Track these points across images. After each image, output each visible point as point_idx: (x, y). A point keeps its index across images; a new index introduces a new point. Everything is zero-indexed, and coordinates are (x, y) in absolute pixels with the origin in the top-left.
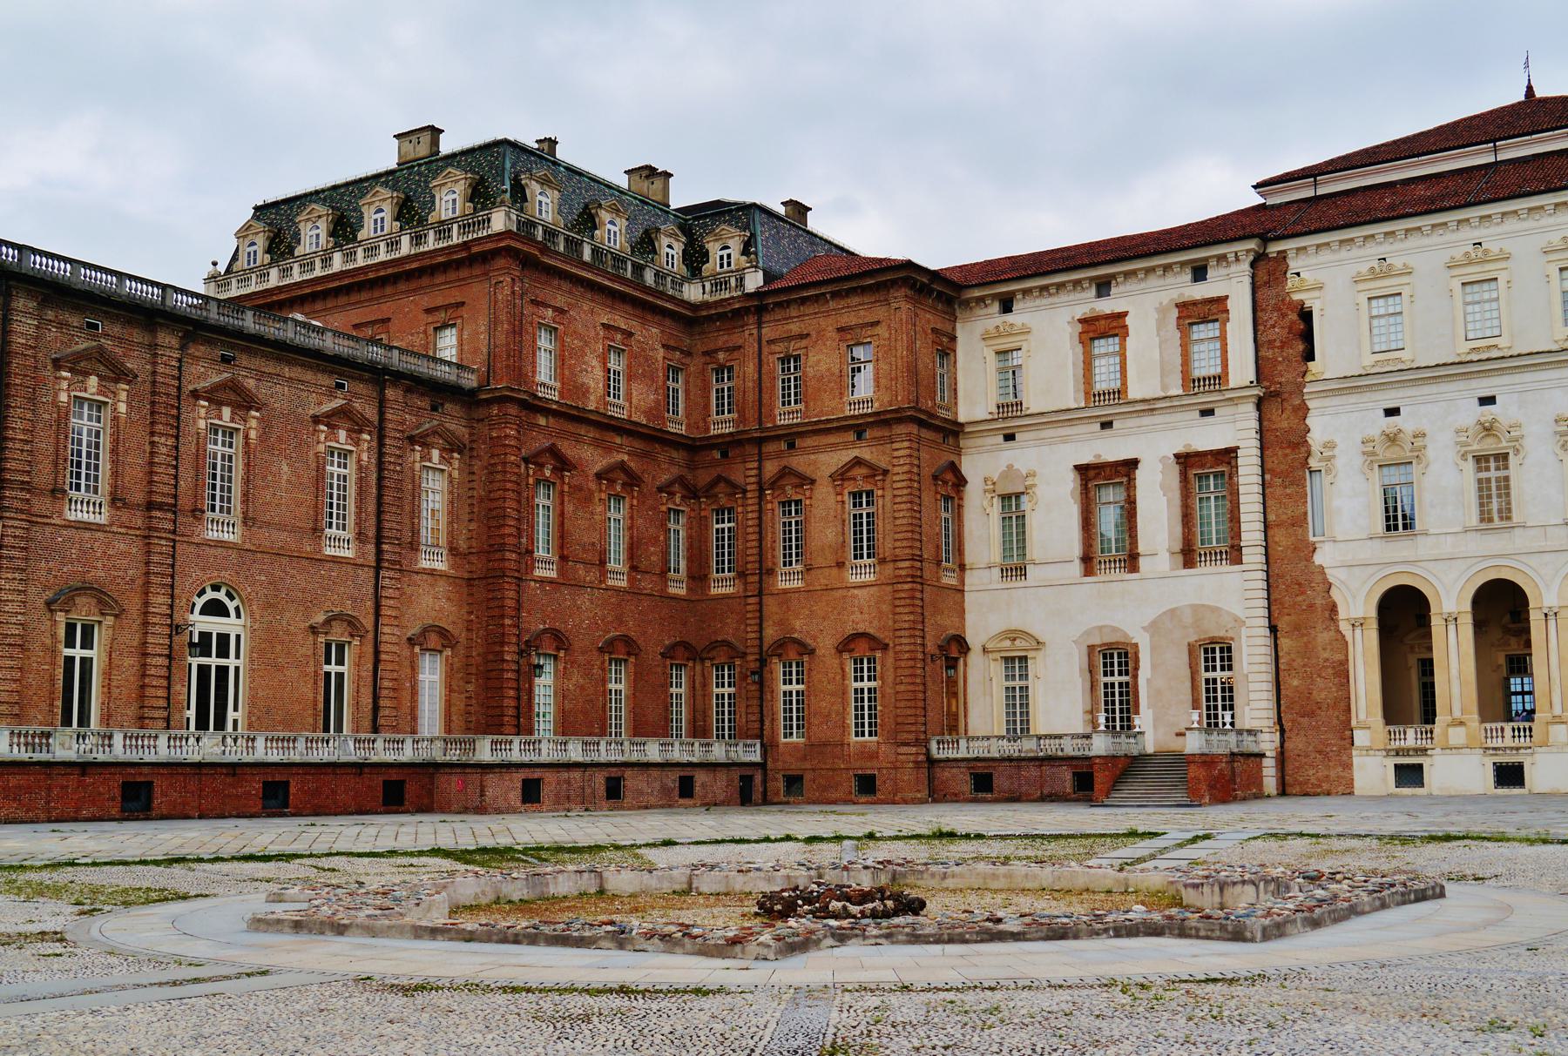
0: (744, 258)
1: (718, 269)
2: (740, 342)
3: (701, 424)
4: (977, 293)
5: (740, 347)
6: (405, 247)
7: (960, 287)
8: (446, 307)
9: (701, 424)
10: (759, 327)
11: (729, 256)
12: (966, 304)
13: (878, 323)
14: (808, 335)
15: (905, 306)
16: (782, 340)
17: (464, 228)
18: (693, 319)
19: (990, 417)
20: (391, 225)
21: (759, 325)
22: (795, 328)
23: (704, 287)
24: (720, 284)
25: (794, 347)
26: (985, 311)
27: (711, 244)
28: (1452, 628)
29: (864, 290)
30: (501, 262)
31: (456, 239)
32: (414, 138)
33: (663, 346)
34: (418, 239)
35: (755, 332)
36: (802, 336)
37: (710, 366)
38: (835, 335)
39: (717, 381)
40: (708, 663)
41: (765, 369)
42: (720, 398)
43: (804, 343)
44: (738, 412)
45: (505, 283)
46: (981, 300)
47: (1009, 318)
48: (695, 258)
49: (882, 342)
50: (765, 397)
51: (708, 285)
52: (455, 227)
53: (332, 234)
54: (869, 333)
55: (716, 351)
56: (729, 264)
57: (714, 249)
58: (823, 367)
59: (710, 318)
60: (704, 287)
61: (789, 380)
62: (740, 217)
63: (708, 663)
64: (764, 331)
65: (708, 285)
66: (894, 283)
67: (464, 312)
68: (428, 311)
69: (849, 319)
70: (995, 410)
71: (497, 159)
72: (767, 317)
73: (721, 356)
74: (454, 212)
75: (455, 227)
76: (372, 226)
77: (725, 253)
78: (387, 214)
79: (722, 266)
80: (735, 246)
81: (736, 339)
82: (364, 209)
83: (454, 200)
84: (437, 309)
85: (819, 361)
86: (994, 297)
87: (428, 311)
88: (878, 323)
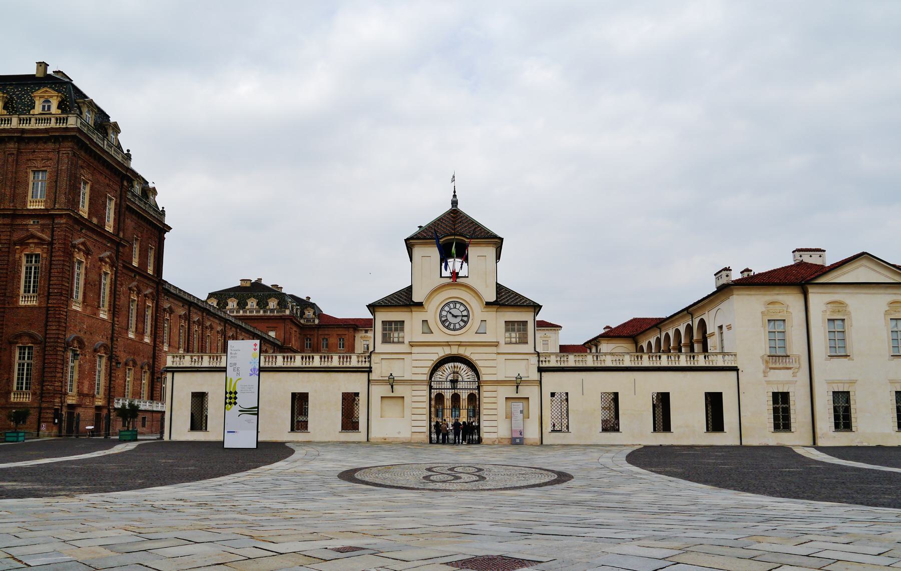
5: (312, 335)
6: (262, 313)
7: (357, 327)
8: (273, 327)
12: (358, 330)
13: (345, 335)
14: (329, 335)
15: (352, 332)
17: (277, 312)
18: (302, 328)
20: (255, 306)
21: (318, 331)
22: (326, 332)
24: (308, 320)
25: (326, 337)
31: (275, 314)
34: (265, 312)
36: (328, 335)
42: (307, 345)
45: (289, 325)
46: (361, 330)
47: (366, 334)
48: (303, 313)
55: (307, 335)
57: (307, 313)
68: (267, 327)
69: (339, 333)
73: (308, 336)
78: (255, 304)
80: (311, 313)
87: (267, 327)
88: (345, 335)
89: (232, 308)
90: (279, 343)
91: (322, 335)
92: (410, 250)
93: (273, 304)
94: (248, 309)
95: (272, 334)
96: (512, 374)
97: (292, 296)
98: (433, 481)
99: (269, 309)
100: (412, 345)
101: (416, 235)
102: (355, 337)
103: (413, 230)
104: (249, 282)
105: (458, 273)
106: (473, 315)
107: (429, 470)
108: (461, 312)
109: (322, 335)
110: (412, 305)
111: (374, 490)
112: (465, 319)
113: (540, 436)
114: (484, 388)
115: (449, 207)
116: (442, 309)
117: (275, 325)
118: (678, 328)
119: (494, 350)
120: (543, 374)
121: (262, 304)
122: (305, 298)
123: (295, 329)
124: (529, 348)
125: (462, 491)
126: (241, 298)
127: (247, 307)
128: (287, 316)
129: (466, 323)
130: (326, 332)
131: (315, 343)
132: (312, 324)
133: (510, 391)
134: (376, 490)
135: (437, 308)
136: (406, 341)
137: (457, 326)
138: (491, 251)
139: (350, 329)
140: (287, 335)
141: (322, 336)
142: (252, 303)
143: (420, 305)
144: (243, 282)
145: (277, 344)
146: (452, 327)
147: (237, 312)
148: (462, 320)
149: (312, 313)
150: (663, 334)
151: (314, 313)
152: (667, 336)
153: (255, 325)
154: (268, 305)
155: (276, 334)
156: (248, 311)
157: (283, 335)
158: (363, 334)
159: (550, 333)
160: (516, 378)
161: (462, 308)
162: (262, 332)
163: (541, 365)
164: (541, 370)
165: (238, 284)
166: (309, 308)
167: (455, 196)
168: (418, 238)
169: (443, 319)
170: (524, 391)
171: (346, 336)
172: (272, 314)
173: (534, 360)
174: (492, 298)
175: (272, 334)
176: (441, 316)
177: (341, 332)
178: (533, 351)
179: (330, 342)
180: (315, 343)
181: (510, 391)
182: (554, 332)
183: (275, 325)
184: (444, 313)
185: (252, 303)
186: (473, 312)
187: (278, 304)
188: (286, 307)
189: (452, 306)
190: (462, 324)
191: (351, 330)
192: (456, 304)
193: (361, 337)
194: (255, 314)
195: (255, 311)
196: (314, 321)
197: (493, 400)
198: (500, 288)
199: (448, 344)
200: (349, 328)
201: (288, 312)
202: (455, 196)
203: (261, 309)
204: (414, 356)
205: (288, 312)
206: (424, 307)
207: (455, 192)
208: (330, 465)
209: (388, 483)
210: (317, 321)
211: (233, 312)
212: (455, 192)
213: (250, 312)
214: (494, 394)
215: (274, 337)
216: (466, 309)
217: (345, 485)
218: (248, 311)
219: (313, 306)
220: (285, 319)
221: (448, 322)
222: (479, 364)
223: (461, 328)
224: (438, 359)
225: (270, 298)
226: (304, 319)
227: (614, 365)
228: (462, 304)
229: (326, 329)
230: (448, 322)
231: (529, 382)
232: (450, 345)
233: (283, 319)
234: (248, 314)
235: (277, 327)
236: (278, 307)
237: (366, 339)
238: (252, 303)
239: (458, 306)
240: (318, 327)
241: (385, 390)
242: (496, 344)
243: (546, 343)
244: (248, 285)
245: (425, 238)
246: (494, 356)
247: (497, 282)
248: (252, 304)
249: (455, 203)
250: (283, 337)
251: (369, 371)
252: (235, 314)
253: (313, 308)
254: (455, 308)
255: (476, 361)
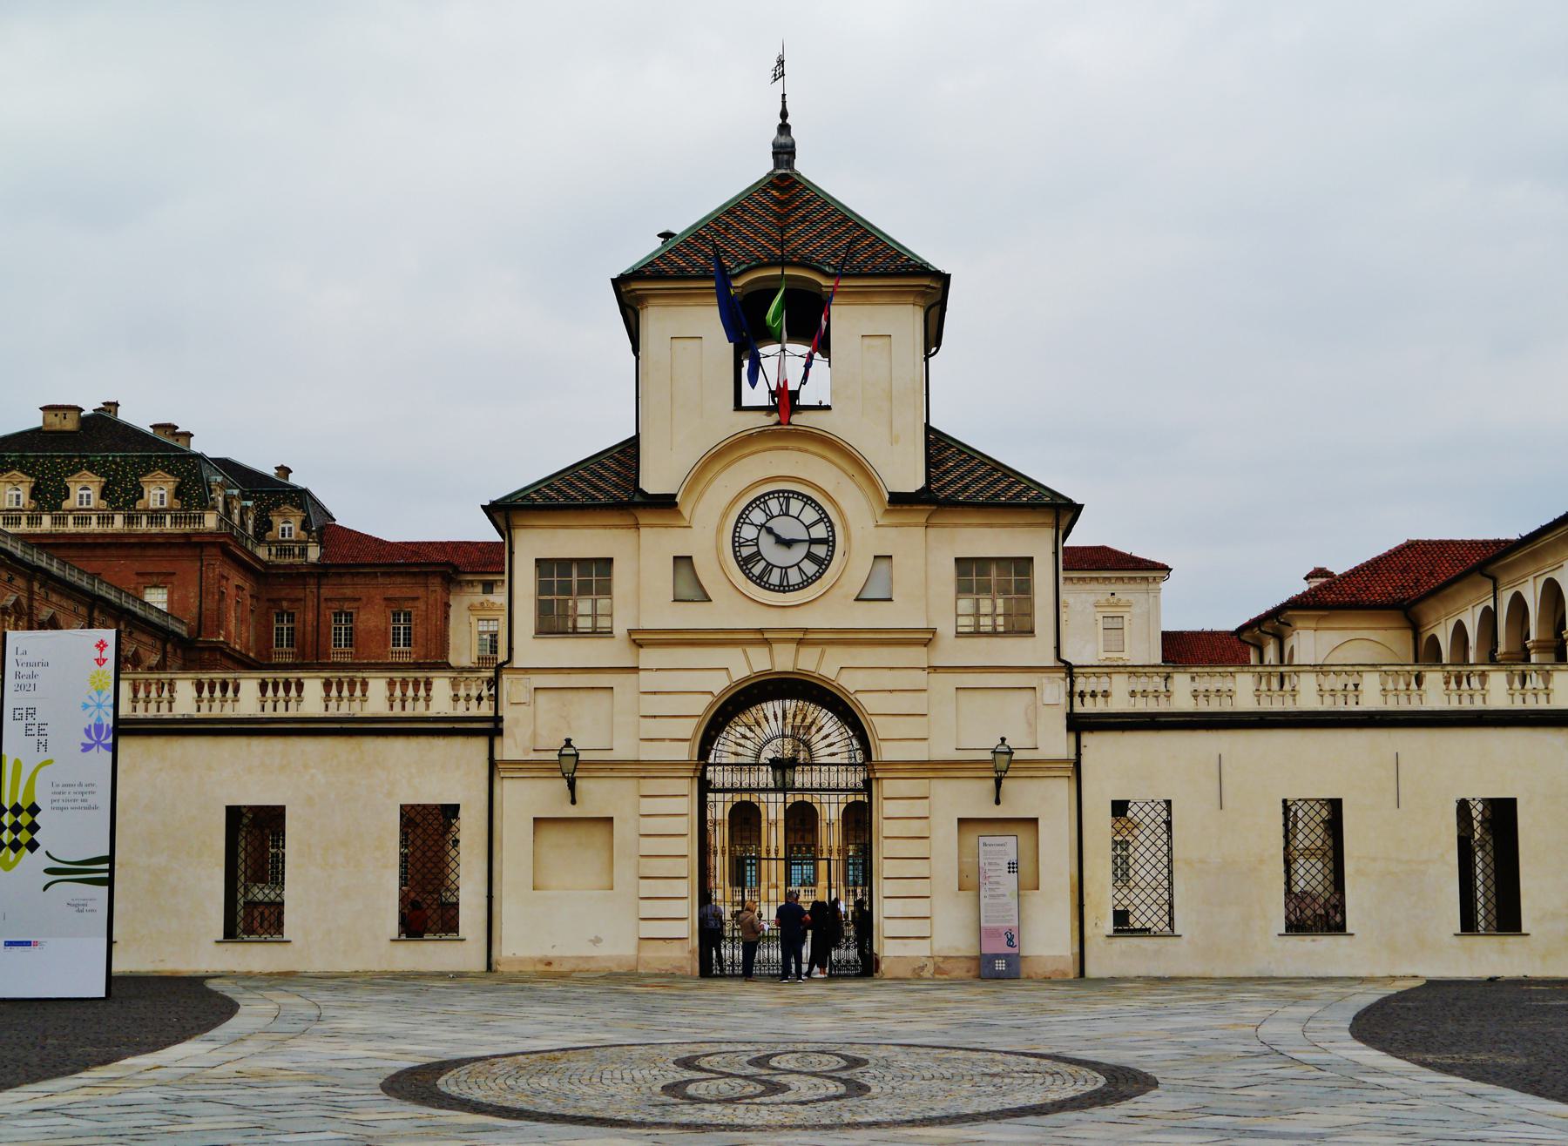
0: (302, 533)
1: (280, 537)
2: (302, 595)
3: (264, 653)
4: (469, 578)
5: (301, 600)
6: (119, 523)
7: (457, 570)
8: (159, 574)
9: (264, 653)
10: (319, 588)
11: (290, 529)
12: (459, 583)
13: (418, 598)
14: (360, 599)
15: (439, 589)
16: (338, 600)
17: (175, 521)
18: (261, 575)
19: (472, 665)
20: (95, 501)
21: (319, 587)
22: (348, 592)
23: (270, 550)
24: (284, 550)
25: (347, 606)
26: (471, 590)
27: (275, 518)
28: (774, 829)
29: (408, 574)
30: (214, 551)
31: (168, 526)
32: (60, 414)
33: (251, 596)
34: (130, 520)
35: (315, 590)
37: (274, 610)
38: (381, 602)
39: (277, 621)
40: (267, 831)
41: (322, 619)
43: (355, 604)
44: (298, 648)
45: (218, 567)
46: (471, 582)
47: (491, 598)
48: (264, 525)
49: (420, 613)
50: (322, 639)
51: (274, 550)
52: (168, 518)
53: (33, 496)
54: (410, 605)
55: (280, 600)
56: (290, 535)
57: (278, 523)
58: (372, 624)
59: (278, 576)
60: (270, 550)
61: (340, 629)
62: (294, 497)
63: (267, 831)
64: (322, 591)
65: (274, 550)
66: (434, 574)
67: (174, 579)
68: (138, 574)
69: (393, 592)
70: (477, 661)
71: (194, 468)
72: (324, 581)
73: (285, 604)
74: (162, 503)
75: (168, 518)
76: (78, 500)
77: (287, 526)
78: (94, 492)
79: (283, 535)
80: (294, 524)
81: (299, 593)
82: (71, 486)
83: (162, 496)
84: (150, 574)
85: (369, 619)
86: (480, 581)
87: (138, 574)
88: (418, 598)
89: (14, 506)
90: (183, 631)
91: (331, 600)
92: (629, 311)
93: (157, 492)
94: (71, 511)
95: (157, 598)
96: (980, 741)
97: (227, 466)
98: (694, 1100)
99: (146, 510)
100: (639, 639)
101: (651, 264)
102: (448, 605)
103: (645, 247)
104: (72, 416)
105: (795, 394)
106: (848, 538)
107: (687, 1063)
108: (808, 528)
109: (331, 600)
110: (636, 505)
111: (497, 1129)
112: (820, 551)
113: (1076, 949)
114: (887, 787)
115: (764, 166)
116: (740, 517)
117: (165, 567)
118: (1556, 576)
119: (917, 656)
120: (1088, 739)
121: (120, 493)
122: (272, 472)
123: (236, 579)
124: (1037, 650)
125: (785, 1131)
126: (43, 472)
127: (66, 504)
128: (211, 534)
129: (823, 564)
130: (348, 592)
131: (309, 629)
132: (298, 561)
133: (973, 798)
134: (505, 1129)
135: (725, 515)
136: (620, 629)
137: (794, 577)
138: (907, 320)
139: (431, 580)
140: (210, 604)
141: (335, 605)
142: (86, 488)
143: (666, 503)
144: (51, 417)
145: (173, 632)
146: (775, 578)
147: (30, 521)
148: (810, 556)
149: (299, 524)
150: (1506, 597)
151: (305, 525)
152: (1518, 603)
153: (96, 565)
154: (141, 497)
155: (170, 595)
156: (70, 518)
157: (193, 602)
158: (476, 596)
159: (1129, 593)
160: (994, 752)
161: (810, 515)
162: (119, 591)
163: (1078, 709)
164: (1078, 725)
165: (35, 420)
166: (285, 508)
167: (784, 128)
168: (660, 276)
169: (746, 552)
170: (1022, 798)
171: (417, 604)
172: (155, 529)
173: (1054, 690)
174: (912, 478)
175: (157, 598)
176: (737, 543)
177: (400, 588)
178: (1050, 661)
179: (361, 626)
180: (309, 629)
181: (973, 798)
182: (1144, 586)
183: (165, 567)
184: (748, 532)
185: (84, 491)
186: (846, 527)
187: (178, 493)
188: (205, 504)
189: (774, 506)
190: (810, 568)
191: (436, 585)
192: (788, 499)
193: (471, 608)
194: (94, 527)
195: (94, 519)
196: (304, 552)
197: (915, 828)
198: (938, 446)
199: (762, 638)
200: (426, 574)
201: (211, 521)
202: (784, 128)
203: (118, 508)
204: (647, 681)
205: (211, 521)
206: (679, 513)
207: (784, 115)
208: (357, 1050)
209: (547, 1106)
210: (314, 553)
211: (18, 521)
212: (784, 115)
213: (77, 521)
214: (918, 808)
215: (163, 607)
216: (824, 518)
217: (406, 1112)
218: (70, 518)
219: (302, 498)
220: (201, 546)
221: (762, 564)
222: (869, 705)
223: (807, 582)
224: (729, 689)
225: (148, 472)
226: (270, 544)
227: (1327, 705)
228: (808, 500)
229: (347, 580)
230: (762, 564)
231: (1039, 767)
232: (767, 642)
233: (193, 545)
234: (71, 527)
235: (174, 574)
236: (177, 504)
237: (487, 615)
238: (84, 491)
239: (795, 506)
240: (321, 572)
241: (546, 796)
242: (926, 638)
243: (1114, 626)
244: (70, 424)
245: (682, 276)
246: (920, 679)
247: (929, 429)
248: (85, 492)
249: (784, 152)
250: (195, 611)
251: (492, 729)
252: (24, 527)
253: (300, 507)
254: (787, 514)
255: (859, 696)
